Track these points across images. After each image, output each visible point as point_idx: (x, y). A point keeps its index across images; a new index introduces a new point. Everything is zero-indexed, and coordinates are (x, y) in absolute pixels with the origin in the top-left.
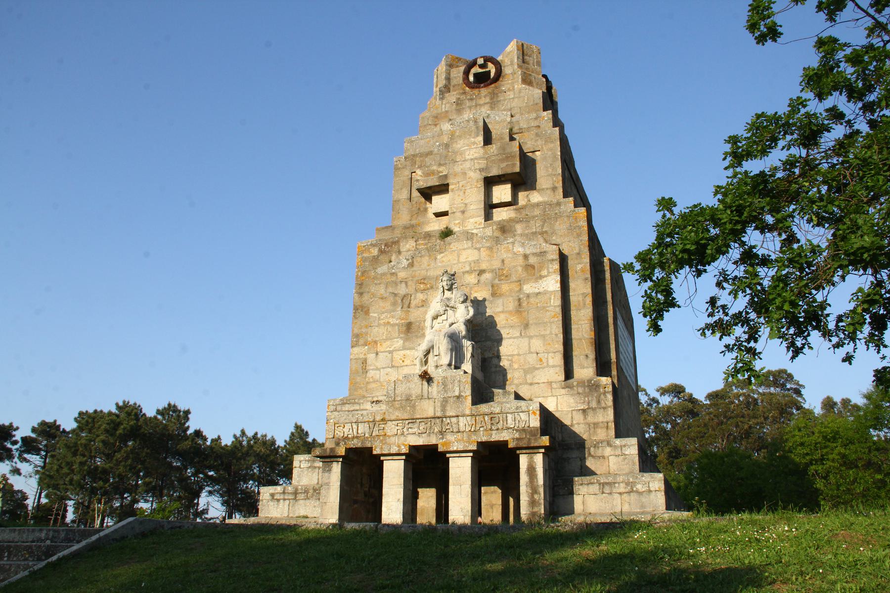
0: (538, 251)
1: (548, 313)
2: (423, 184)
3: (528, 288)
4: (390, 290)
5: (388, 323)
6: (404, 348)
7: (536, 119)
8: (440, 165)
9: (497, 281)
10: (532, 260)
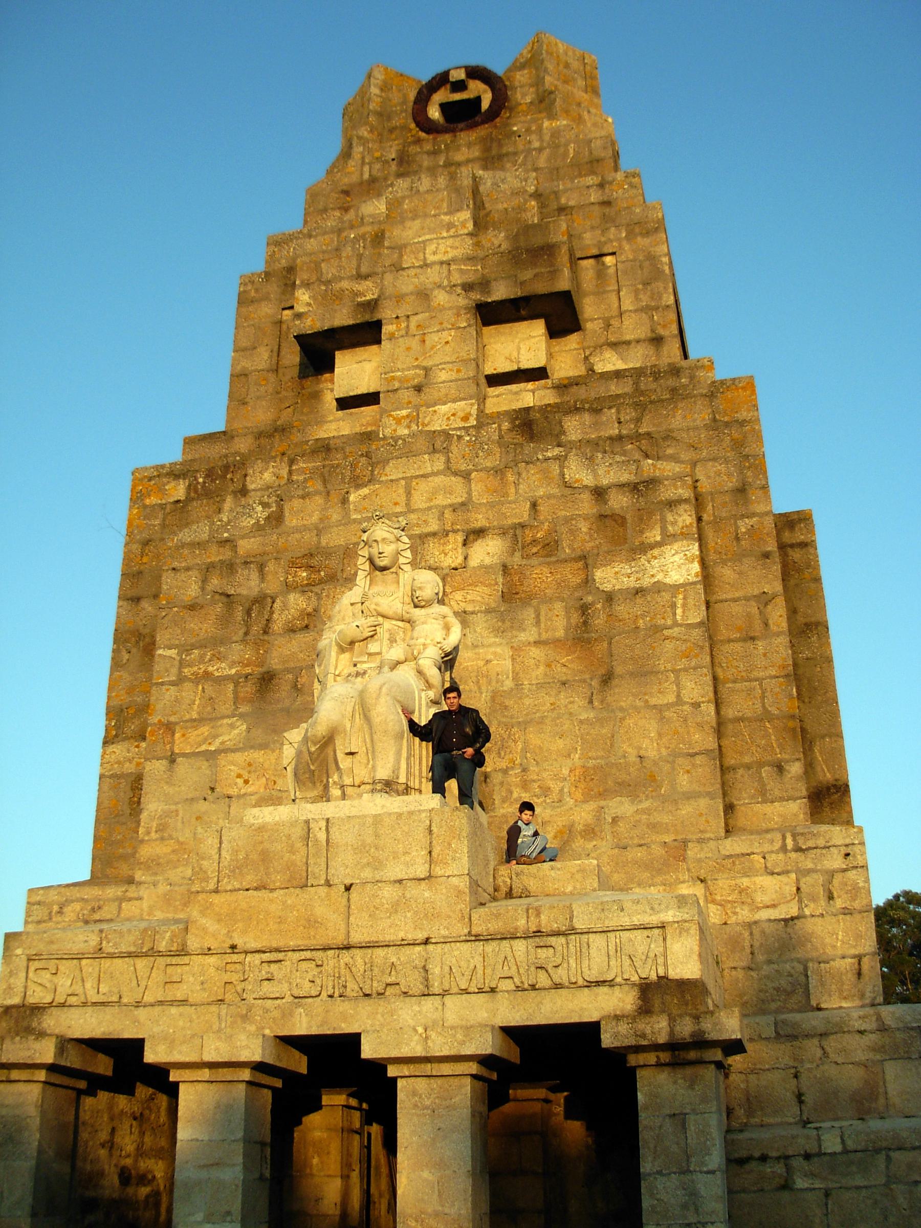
0: (632, 478)
1: (669, 645)
2: (310, 325)
3: (608, 577)
4: (215, 582)
5: (207, 674)
6: (249, 745)
7: (601, 186)
8: (360, 277)
9: (517, 559)
10: (619, 502)
